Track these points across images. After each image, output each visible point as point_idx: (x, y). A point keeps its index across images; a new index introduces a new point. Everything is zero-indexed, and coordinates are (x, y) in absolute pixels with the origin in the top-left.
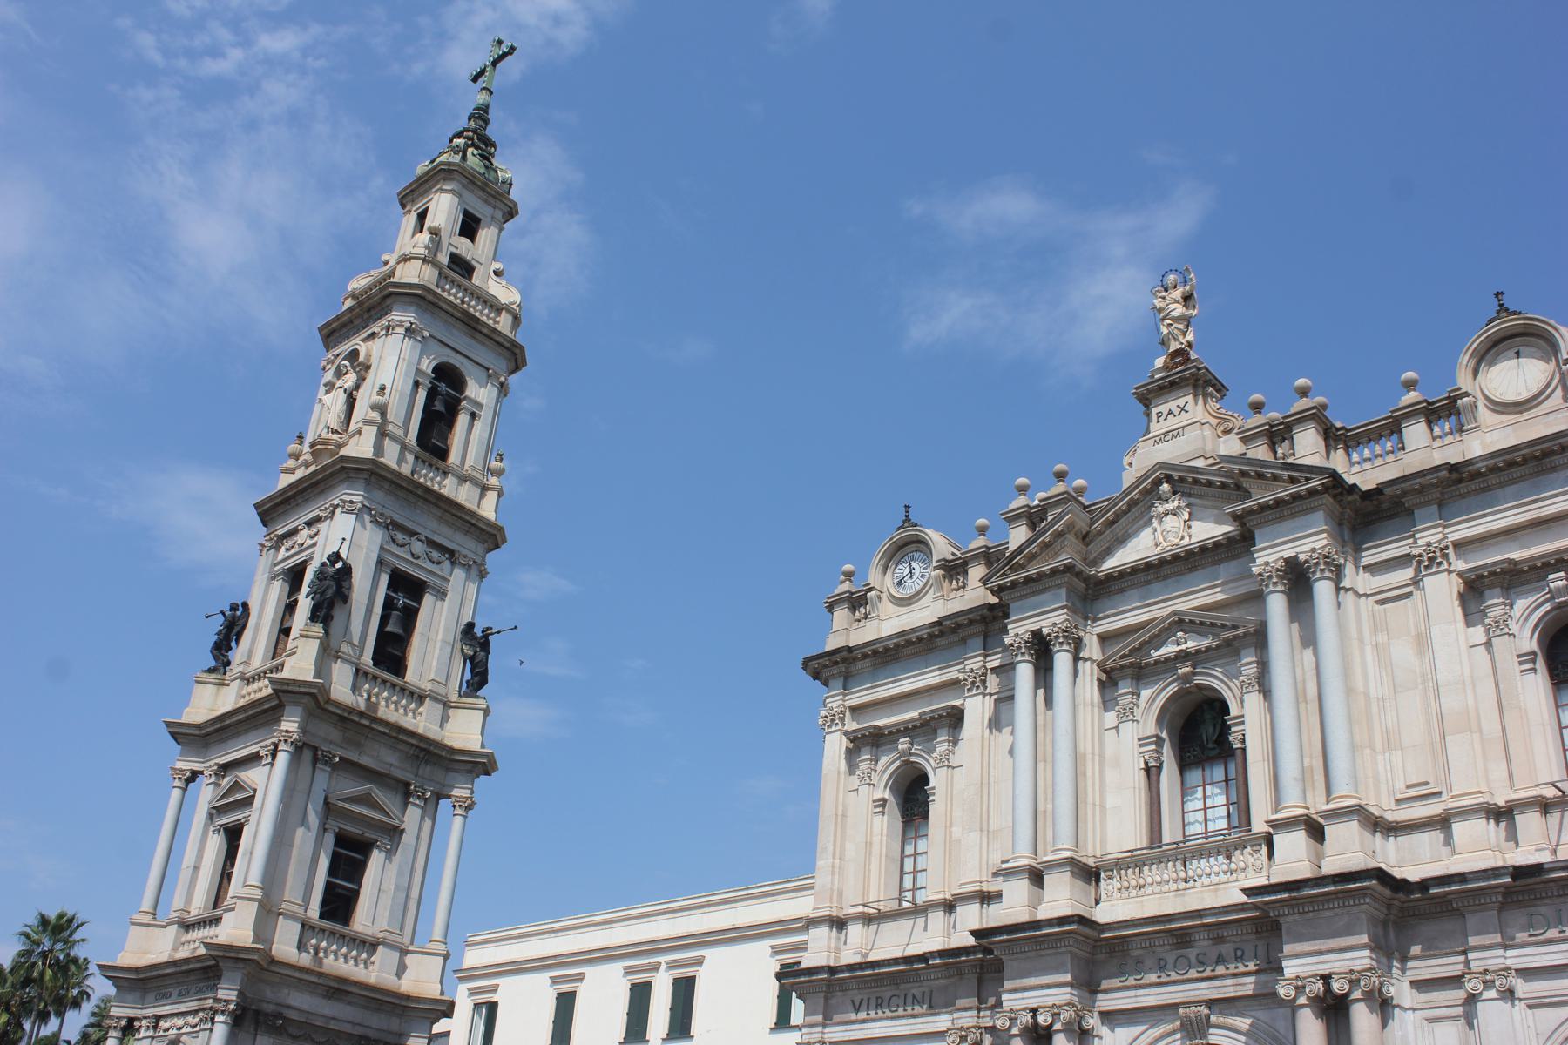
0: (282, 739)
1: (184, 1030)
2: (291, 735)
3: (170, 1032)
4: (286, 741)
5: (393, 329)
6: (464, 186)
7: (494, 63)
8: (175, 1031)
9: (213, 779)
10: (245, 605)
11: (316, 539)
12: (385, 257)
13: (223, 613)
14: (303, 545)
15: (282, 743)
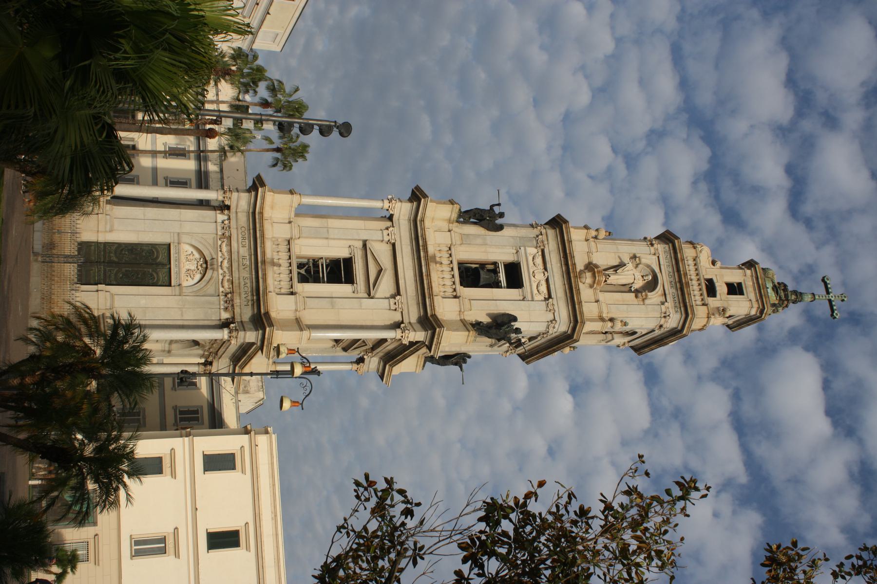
0: (404, 334)
1: (221, 271)
2: (406, 339)
3: (220, 254)
4: (402, 337)
5: (665, 317)
6: (751, 316)
7: (830, 301)
8: (220, 260)
9: (386, 238)
10: (500, 228)
11: (535, 291)
12: (718, 264)
13: (499, 205)
14: (534, 277)
15: (401, 335)
